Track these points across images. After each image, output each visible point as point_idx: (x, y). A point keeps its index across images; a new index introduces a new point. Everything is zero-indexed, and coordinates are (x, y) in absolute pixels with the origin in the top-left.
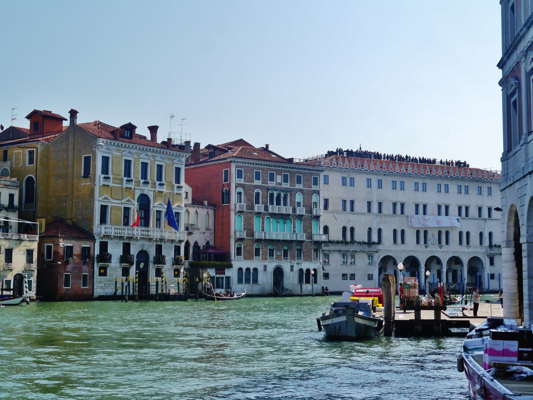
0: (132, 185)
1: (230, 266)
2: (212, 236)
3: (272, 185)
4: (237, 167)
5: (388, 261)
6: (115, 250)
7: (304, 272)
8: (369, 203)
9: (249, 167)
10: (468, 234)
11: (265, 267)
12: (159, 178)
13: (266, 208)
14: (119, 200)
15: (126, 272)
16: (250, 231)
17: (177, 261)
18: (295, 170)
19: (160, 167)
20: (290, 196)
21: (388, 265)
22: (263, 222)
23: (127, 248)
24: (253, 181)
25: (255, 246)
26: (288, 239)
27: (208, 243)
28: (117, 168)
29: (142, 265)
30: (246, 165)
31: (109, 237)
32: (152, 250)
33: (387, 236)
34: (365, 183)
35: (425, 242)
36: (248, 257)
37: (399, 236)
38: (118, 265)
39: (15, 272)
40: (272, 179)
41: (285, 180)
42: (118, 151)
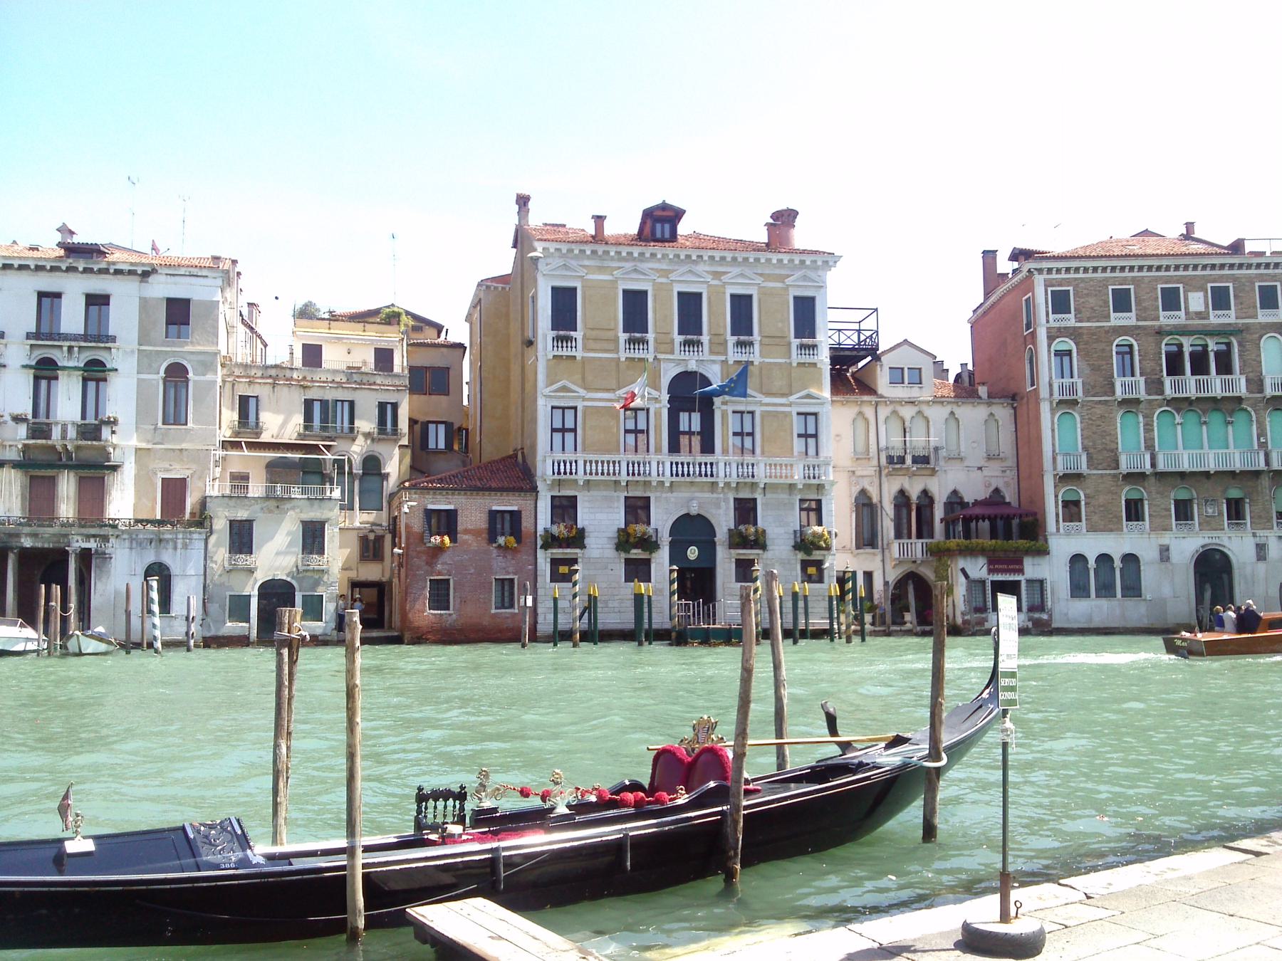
1: (1043, 552)
2: (1011, 474)
3: (1172, 322)
4: (1048, 284)
6: (599, 516)
9: (1091, 279)
11: (1164, 552)
13: (1155, 386)
14: (608, 390)
16: (1106, 454)
18: (1253, 271)
20: (1240, 344)
22: (1148, 428)
23: (638, 508)
24: (1107, 318)
25: (1126, 492)
26: (1237, 466)
29: (693, 553)
30: (1081, 275)
32: (721, 511)
36: (1105, 524)
38: (610, 552)
39: (261, 577)
42: (601, 269)
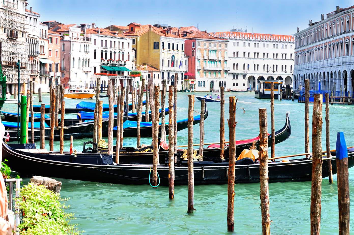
0: (170, 52)
2: (188, 68)
5: (252, 79)
7: (221, 83)
8: (244, 53)
10: (286, 66)
12: (177, 49)
17: (182, 79)
19: (177, 45)
21: (251, 79)
23: (169, 73)
27: (186, 71)
29: (172, 80)
31: (164, 71)
33: (251, 67)
34: (243, 44)
35: (267, 70)
36: (202, 76)
37: (256, 67)
40: (210, 46)
41: (215, 46)
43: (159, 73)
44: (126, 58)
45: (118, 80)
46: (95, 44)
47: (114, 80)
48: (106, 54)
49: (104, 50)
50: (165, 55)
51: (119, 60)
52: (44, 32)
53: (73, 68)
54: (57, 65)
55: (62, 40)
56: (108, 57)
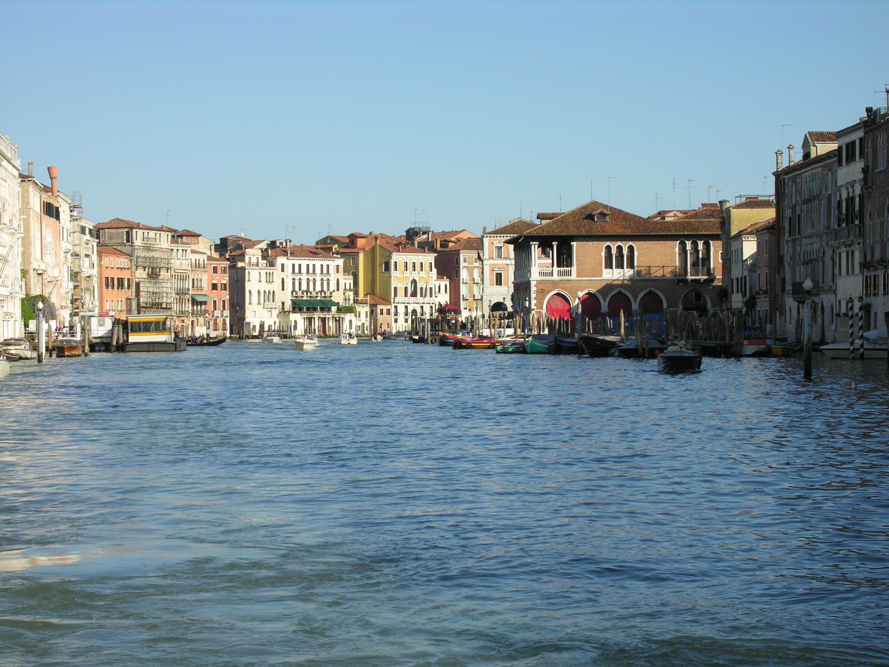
15: (406, 321)
23: (406, 307)
28: (401, 266)
43: (388, 307)
44: (333, 286)
45: (316, 319)
46: (283, 270)
47: (310, 320)
48: (300, 283)
49: (297, 278)
50: (399, 280)
51: (322, 291)
52: (202, 262)
53: (250, 304)
54: (224, 301)
55: (233, 267)
56: (304, 287)
